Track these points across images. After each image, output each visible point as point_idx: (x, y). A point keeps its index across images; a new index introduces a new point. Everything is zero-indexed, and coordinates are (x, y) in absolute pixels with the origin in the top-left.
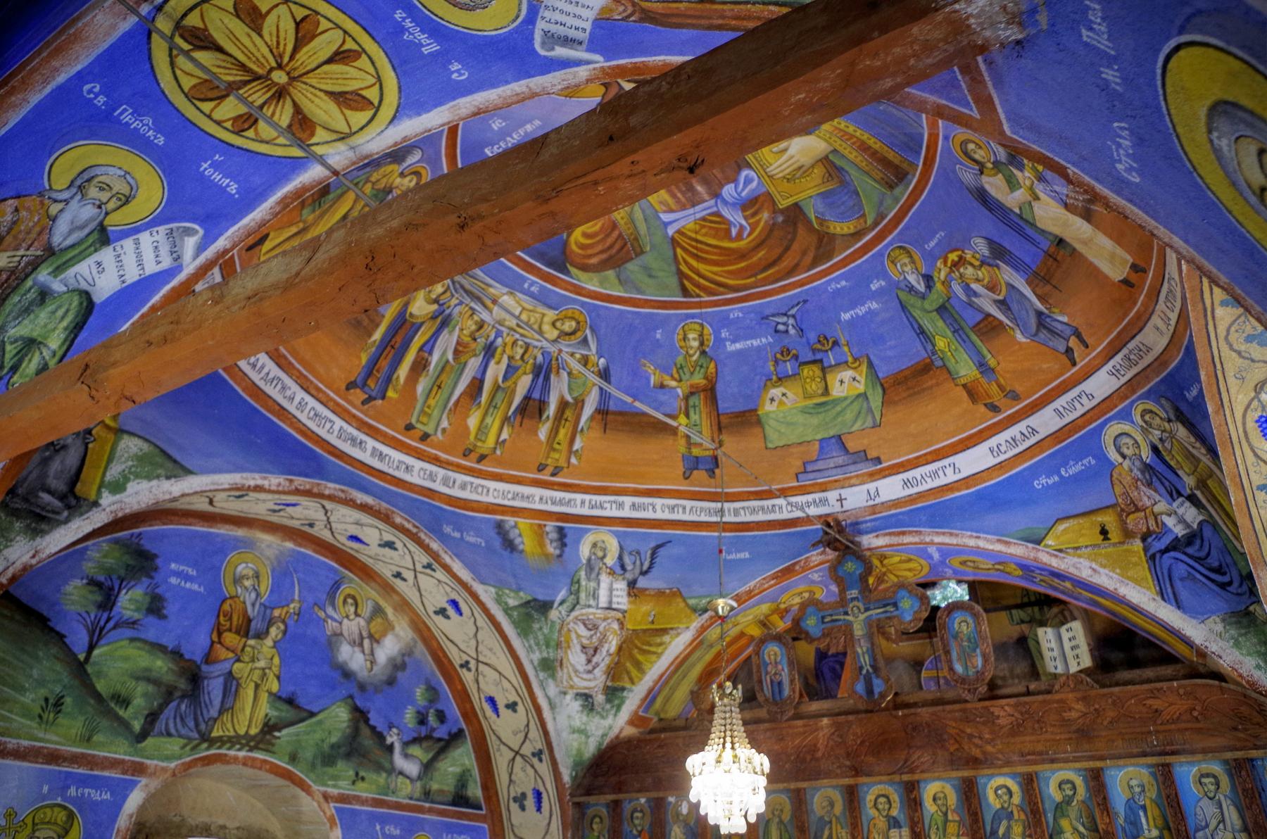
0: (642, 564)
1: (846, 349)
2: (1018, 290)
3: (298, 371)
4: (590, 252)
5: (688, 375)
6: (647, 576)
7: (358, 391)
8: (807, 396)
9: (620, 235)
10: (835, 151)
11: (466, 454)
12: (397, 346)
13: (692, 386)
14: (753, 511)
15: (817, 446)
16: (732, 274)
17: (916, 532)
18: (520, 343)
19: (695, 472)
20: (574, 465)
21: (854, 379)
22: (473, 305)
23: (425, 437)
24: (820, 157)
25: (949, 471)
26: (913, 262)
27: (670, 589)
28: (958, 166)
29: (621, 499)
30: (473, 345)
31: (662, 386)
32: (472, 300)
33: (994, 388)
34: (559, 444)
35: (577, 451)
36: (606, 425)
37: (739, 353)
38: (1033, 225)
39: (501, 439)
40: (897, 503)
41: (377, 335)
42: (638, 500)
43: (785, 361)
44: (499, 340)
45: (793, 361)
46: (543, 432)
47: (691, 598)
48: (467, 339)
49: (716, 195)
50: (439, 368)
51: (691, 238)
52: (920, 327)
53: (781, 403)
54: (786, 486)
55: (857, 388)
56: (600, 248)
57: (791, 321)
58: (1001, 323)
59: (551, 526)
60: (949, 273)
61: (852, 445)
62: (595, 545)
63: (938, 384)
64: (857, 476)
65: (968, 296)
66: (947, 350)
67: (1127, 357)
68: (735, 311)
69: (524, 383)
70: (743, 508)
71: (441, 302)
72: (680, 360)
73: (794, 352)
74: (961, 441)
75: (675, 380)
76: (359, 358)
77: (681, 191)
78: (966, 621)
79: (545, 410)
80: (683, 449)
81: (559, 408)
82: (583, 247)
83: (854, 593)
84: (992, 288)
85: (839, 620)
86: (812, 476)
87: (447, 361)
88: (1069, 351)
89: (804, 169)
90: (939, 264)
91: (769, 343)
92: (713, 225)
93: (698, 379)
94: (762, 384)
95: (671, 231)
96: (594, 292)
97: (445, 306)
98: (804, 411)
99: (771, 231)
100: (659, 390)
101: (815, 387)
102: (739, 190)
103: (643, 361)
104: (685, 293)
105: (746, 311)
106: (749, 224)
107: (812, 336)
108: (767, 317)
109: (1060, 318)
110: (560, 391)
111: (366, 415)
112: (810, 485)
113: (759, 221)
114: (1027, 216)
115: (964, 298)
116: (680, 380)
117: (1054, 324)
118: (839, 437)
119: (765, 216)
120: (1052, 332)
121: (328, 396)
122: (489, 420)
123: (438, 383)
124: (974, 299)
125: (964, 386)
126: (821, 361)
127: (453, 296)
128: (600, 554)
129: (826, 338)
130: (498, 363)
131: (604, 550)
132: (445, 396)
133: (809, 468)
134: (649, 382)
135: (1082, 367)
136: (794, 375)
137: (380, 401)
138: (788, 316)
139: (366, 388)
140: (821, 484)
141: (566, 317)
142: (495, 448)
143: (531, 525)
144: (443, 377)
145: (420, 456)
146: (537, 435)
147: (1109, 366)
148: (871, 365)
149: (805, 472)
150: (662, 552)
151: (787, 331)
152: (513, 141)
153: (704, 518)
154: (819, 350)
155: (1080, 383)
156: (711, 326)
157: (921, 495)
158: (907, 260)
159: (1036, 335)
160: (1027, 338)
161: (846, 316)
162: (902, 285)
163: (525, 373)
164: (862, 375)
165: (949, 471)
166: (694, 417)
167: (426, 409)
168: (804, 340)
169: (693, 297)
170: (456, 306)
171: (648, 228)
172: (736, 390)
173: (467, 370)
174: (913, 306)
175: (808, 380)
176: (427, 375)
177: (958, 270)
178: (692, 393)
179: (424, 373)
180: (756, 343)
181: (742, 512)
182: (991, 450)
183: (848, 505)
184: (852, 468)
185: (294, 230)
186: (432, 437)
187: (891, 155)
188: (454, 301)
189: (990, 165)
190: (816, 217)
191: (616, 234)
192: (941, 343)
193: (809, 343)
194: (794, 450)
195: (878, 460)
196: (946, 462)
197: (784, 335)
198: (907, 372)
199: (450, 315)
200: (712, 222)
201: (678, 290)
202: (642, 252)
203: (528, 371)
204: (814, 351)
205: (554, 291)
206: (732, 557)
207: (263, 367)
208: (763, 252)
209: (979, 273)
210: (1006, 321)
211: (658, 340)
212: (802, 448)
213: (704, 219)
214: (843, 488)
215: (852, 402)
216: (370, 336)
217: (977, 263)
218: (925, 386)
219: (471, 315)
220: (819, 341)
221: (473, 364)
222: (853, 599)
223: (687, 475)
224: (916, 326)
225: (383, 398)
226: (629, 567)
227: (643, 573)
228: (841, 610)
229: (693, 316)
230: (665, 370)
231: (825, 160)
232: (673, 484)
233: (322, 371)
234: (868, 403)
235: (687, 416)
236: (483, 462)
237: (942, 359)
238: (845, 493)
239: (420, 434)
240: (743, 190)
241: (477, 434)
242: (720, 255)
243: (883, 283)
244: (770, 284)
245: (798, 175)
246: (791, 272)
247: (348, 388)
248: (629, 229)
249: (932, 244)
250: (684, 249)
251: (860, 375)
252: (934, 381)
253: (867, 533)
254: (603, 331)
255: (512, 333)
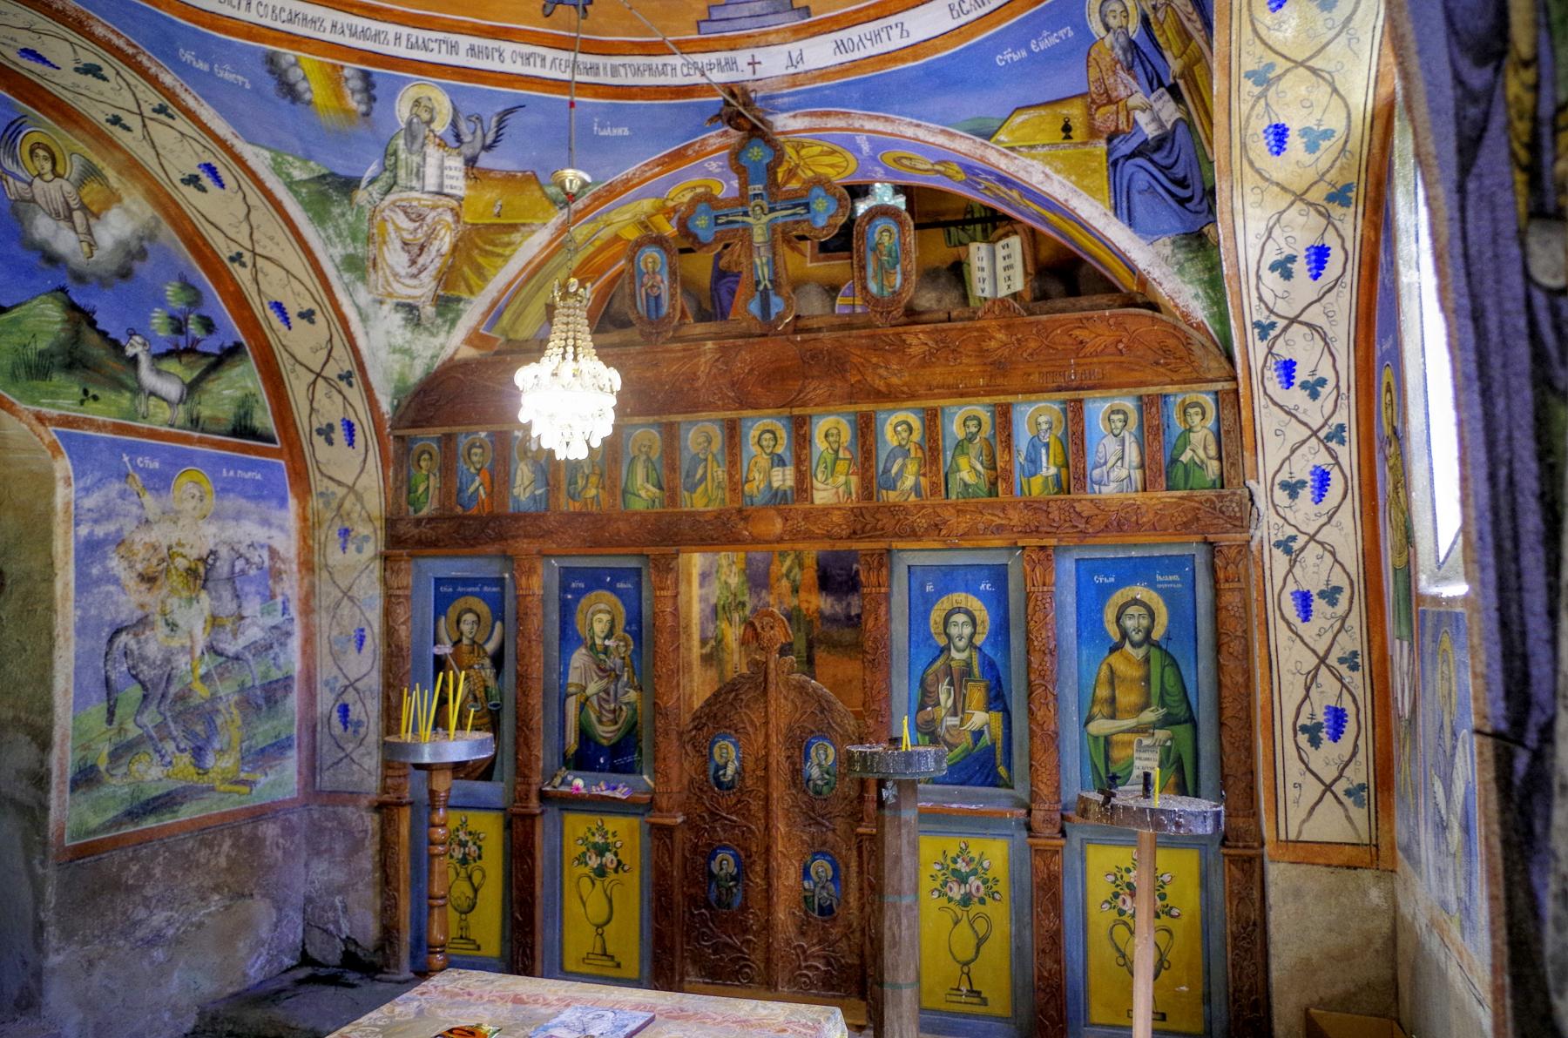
0: (484, 136)
6: (494, 152)
14: (638, 71)
19: (559, 6)
25: (895, 32)
29: (453, 37)
40: (823, 73)
42: (478, 42)
47: (550, 185)
59: (350, 68)
62: (417, 103)
64: (777, 31)
70: (624, 65)
78: (888, 231)
83: (757, 188)
86: (716, 26)
112: (714, 39)
128: (426, 116)
131: (431, 110)
133: (716, 15)
140: (729, 38)
143: (322, 63)
150: (512, 119)
157: (856, 65)
165: (895, 32)
181: (622, 71)
184: (771, 19)
195: (807, 11)
196: (892, 20)
222: (756, 196)
223: (548, 10)
226: (467, 138)
228: (740, 209)
238: (760, 54)
253: (783, 111)
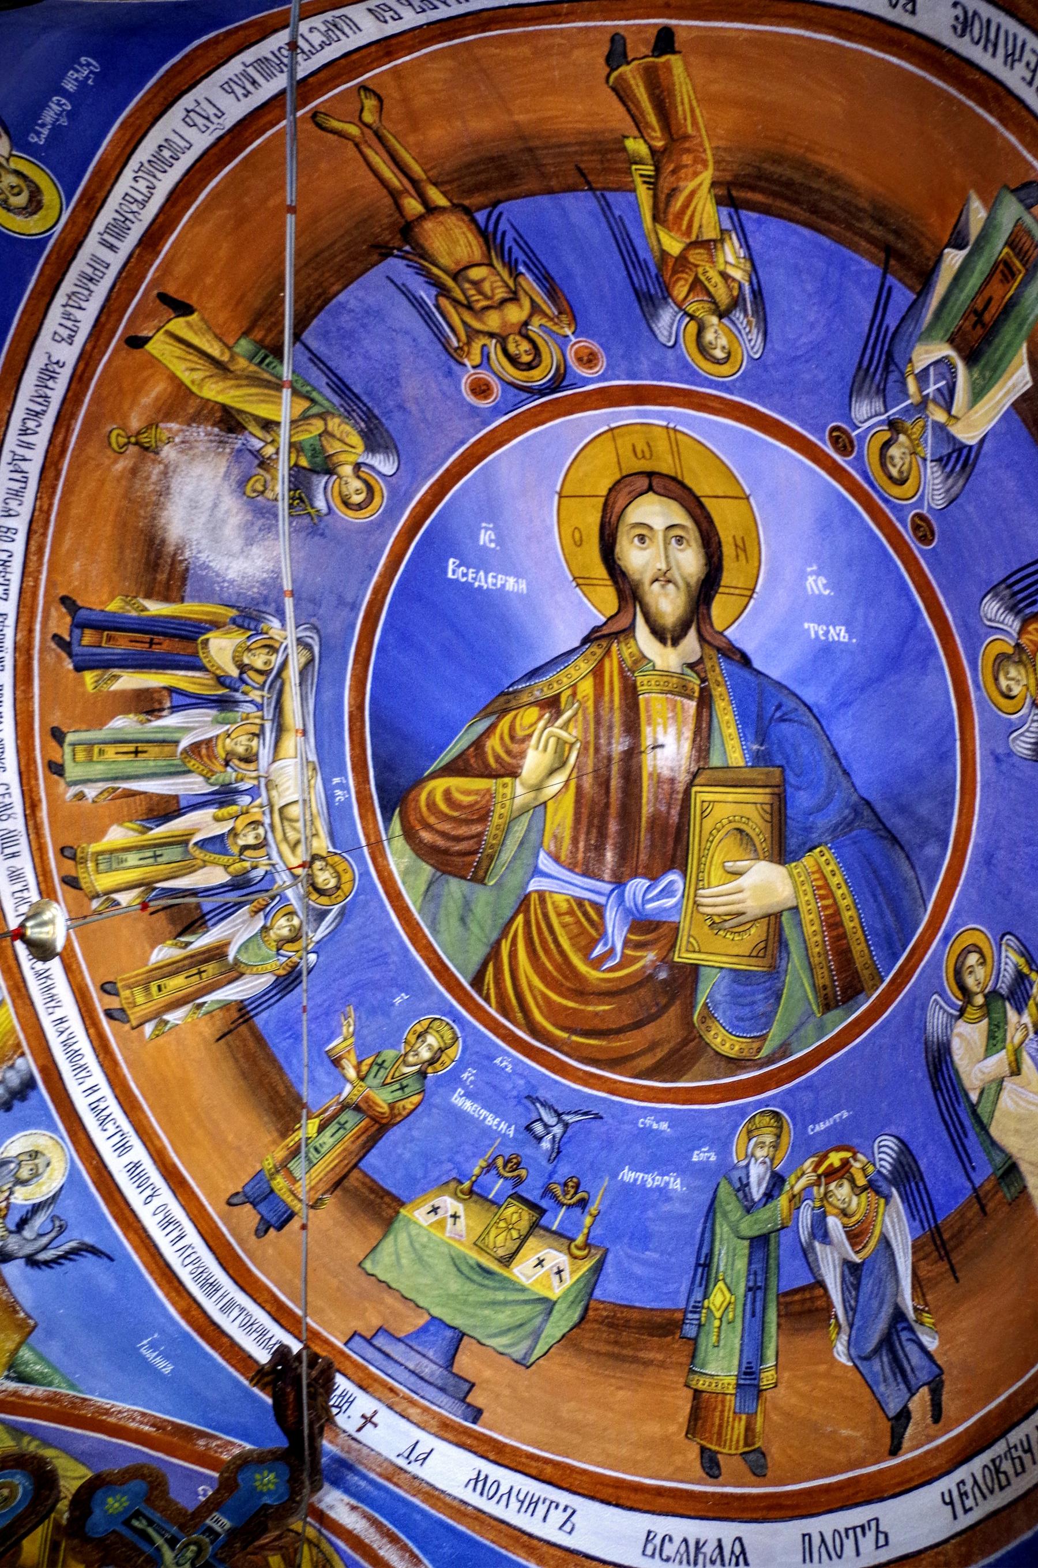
0: (45, 1248)
1: (588, 1220)
2: (893, 1255)
3: (51, 505)
4: (432, 820)
5: (378, 1081)
6: (30, 1271)
7: (68, 619)
8: (479, 1245)
9: (480, 835)
10: (795, 909)
11: (66, 852)
12: (156, 649)
13: (367, 1099)
14: (249, 1326)
15: (421, 1322)
16: (552, 1011)
17: (413, 1555)
18: (261, 831)
19: (249, 1206)
20: (142, 1033)
21: (559, 1272)
22: (268, 725)
23: (56, 769)
24: (770, 911)
25: (557, 1517)
26: (776, 1146)
27: (29, 1317)
28: (935, 996)
29: (134, 1140)
30: (218, 766)
31: (336, 1062)
32: (273, 720)
33: (740, 1427)
34: (160, 989)
35: (166, 1022)
36: (230, 1032)
37: (459, 1115)
38: (984, 1128)
39: (115, 896)
40: (434, 1494)
41: (156, 608)
42: (149, 1166)
43: (500, 1176)
44: (247, 799)
45: (509, 1184)
46: (163, 953)
47: (32, 1349)
48: (220, 752)
49: (619, 882)
50: (160, 736)
51: (546, 916)
52: (710, 1255)
53: (441, 1224)
54: (325, 1334)
55: (550, 1288)
56: (446, 827)
57: (558, 1130)
58: (830, 1305)
59: (27, 1064)
60: (811, 1185)
61: (466, 1363)
62: (34, 1154)
63: (662, 1365)
64: (425, 1410)
65: (813, 1235)
66: (718, 1314)
67: (995, 1468)
68: (508, 1058)
69: (214, 876)
70: (243, 1309)
71: (245, 676)
72: (389, 1054)
73: (523, 1173)
74: (619, 1484)
75: (358, 1072)
76: (112, 598)
77: (587, 840)
79: (194, 933)
80: (269, 1164)
81: (209, 950)
82: (431, 805)
83: (220, 1523)
84: (855, 1236)
85: (151, 1541)
86: (370, 1353)
87: (177, 742)
88: (904, 1416)
89: (742, 919)
90: (808, 1164)
91: (505, 1136)
92: (583, 920)
93: (382, 1099)
94: (444, 1179)
95: (533, 886)
96: (390, 873)
97: (244, 688)
98: (457, 1262)
99: (640, 984)
100: (327, 1061)
101: (501, 1241)
102: (649, 896)
103: (351, 1010)
104: (478, 981)
105: (519, 1071)
106: (623, 954)
107: (564, 1170)
108: (534, 1100)
109: (926, 1340)
110: (234, 934)
111: (41, 652)
112: (354, 1363)
113: (638, 959)
114: (983, 1111)
115: (804, 1236)
116: (362, 1079)
117: (911, 1349)
118: (460, 1336)
119: (650, 956)
120: (898, 1366)
121: (40, 572)
122: (132, 859)
123: (141, 747)
124: (817, 1244)
125: (697, 1393)
126: (542, 1212)
127: (262, 688)
128: (24, 1173)
129: (577, 1186)
130: (217, 819)
131: (36, 1174)
132: (130, 770)
133: (380, 1341)
134: (330, 1040)
135: (906, 1463)
136: (493, 1202)
137: (71, 667)
138: (560, 1120)
139: (77, 631)
140: (371, 1375)
141: (333, 866)
142: (97, 896)
143: (13, 1030)
144: (154, 750)
145: (26, 774)
146: (153, 948)
147: (948, 1483)
148: (598, 1269)
149: (369, 1342)
150: (88, 1263)
151: (540, 1139)
152: (483, 584)
153: (185, 1275)
154: (555, 1197)
155: (882, 1499)
156: (464, 1051)
157: (480, 1517)
158: (769, 1139)
159: (866, 1359)
160: (851, 1358)
161: (628, 1175)
162: (735, 1175)
163: (226, 867)
164: (575, 1273)
165: (557, 1517)
166: (327, 1139)
167: (96, 749)
168: (550, 1167)
169: (480, 994)
170: (252, 702)
171: (514, 858)
172: (407, 1155)
173: (180, 780)
174: (725, 1215)
175: (502, 1224)
176: (142, 723)
177: (827, 1184)
178: (357, 1108)
179: (143, 717)
180: (491, 1121)
181: (236, 1312)
182: (649, 1536)
183: (368, 1436)
184: (431, 1392)
185: (215, 350)
186: (62, 782)
187: (858, 949)
188: (255, 695)
189: (979, 1000)
190: (706, 1004)
191: (476, 828)
192: (718, 1297)
193: (550, 1177)
194: (389, 1300)
195: (476, 1414)
196: (564, 1498)
197: (535, 1141)
198: (635, 1315)
199: (236, 703)
200: (585, 914)
201: (473, 967)
202: (482, 881)
203: (231, 869)
204: (547, 1192)
205: (354, 825)
206: (149, 1355)
207: (29, 446)
208: (607, 1008)
209: (855, 1199)
210: (839, 1309)
211: (393, 1004)
212: (399, 1306)
213: (580, 902)
214: (390, 1407)
215: (526, 1302)
216: (148, 596)
217: (861, 1181)
218: (641, 1354)
219: (254, 734)
220: (565, 1184)
221: (193, 785)
222: (210, 1531)
223: (235, 1201)
224: (705, 1251)
225: (79, 669)
226: (27, 1233)
227: (31, 1261)
228: (175, 1529)
229: (457, 1019)
230: (362, 1050)
231: (774, 919)
232: (208, 1196)
233: (67, 544)
234: (546, 1321)
235: (321, 1129)
236: (66, 887)
237: (700, 1326)
238: (385, 1416)
239: (57, 758)
240: (652, 900)
241: (101, 853)
242: (558, 968)
243: (713, 1158)
244: (577, 1060)
245: (727, 925)
246: (612, 1064)
247: (65, 600)
248: (495, 837)
249: (821, 1127)
250: (527, 923)
251: (572, 1272)
252: (660, 1357)
253: (347, 1491)
254: (349, 926)
255: (267, 809)
